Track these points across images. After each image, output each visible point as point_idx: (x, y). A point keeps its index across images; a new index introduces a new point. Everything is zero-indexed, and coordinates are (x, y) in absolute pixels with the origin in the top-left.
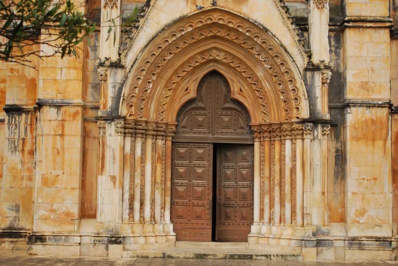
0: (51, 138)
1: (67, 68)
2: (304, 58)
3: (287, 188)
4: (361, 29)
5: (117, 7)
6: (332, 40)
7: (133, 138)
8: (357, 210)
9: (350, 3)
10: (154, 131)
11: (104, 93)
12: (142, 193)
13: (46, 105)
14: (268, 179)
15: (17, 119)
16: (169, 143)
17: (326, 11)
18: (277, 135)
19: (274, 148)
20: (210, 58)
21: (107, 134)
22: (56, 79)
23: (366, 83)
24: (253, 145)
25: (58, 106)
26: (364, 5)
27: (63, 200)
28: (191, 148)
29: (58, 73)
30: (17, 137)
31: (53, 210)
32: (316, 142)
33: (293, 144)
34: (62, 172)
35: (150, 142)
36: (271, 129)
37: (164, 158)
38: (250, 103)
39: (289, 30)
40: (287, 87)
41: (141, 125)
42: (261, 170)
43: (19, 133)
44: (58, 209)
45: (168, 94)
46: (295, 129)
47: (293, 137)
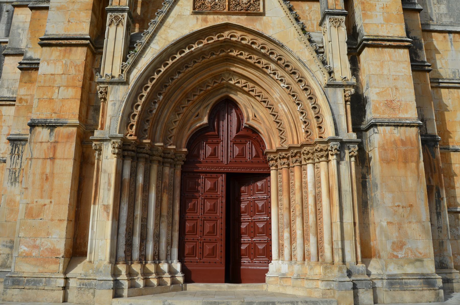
0: (40, 161)
1: (65, 86)
3: (311, 218)
4: (380, 49)
7: (135, 163)
8: (394, 243)
9: (367, 24)
10: (160, 156)
12: (144, 227)
13: (38, 126)
14: (288, 210)
15: (20, 149)
16: (178, 173)
17: (343, 29)
18: (297, 161)
19: (294, 175)
22: (53, 98)
23: (391, 101)
24: (269, 175)
25: (52, 126)
26: (380, 25)
27: (48, 234)
29: (55, 92)
30: (18, 167)
31: (35, 245)
34: (49, 200)
37: (172, 188)
42: (278, 200)
43: (21, 163)
44: (42, 246)
45: (176, 118)
47: (317, 160)
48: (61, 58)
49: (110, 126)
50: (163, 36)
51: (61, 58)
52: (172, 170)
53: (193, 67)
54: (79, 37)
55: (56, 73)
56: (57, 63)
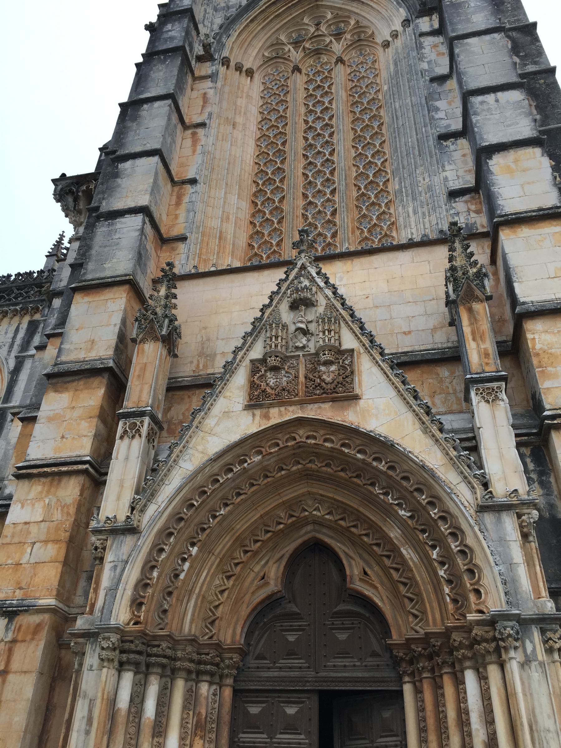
1: (43, 541)
2: (473, 487)
5: (140, 436)
6: (528, 460)
7: (141, 676)
9: (548, 389)
10: (191, 661)
11: (95, 583)
16: (228, 693)
19: (443, 695)
20: (302, 515)
21: (86, 666)
22: (21, 562)
24: (400, 694)
28: (273, 703)
32: (535, 675)
33: (483, 678)
35: (180, 687)
36: (430, 649)
38: (385, 598)
39: (437, 440)
40: (446, 548)
41: (158, 646)
46: (478, 639)
48: (44, 495)
49: (103, 607)
50: (200, 448)
51: (44, 495)
52: (214, 687)
53: (249, 493)
54: (73, 459)
55: (32, 521)
56: (37, 504)
